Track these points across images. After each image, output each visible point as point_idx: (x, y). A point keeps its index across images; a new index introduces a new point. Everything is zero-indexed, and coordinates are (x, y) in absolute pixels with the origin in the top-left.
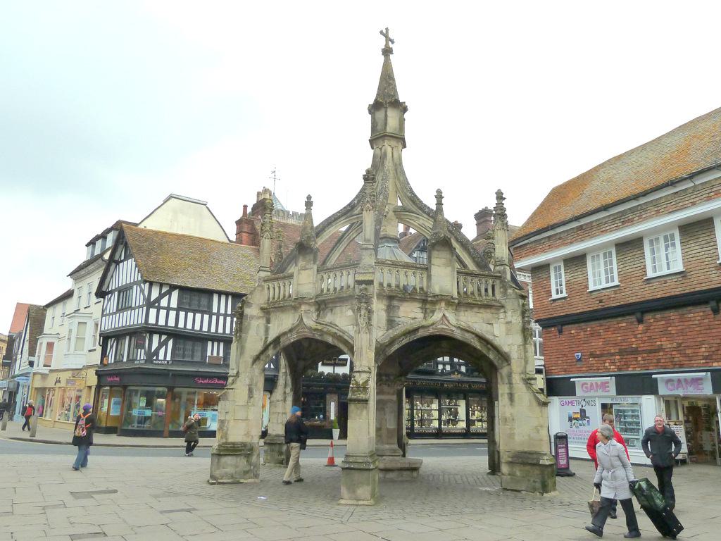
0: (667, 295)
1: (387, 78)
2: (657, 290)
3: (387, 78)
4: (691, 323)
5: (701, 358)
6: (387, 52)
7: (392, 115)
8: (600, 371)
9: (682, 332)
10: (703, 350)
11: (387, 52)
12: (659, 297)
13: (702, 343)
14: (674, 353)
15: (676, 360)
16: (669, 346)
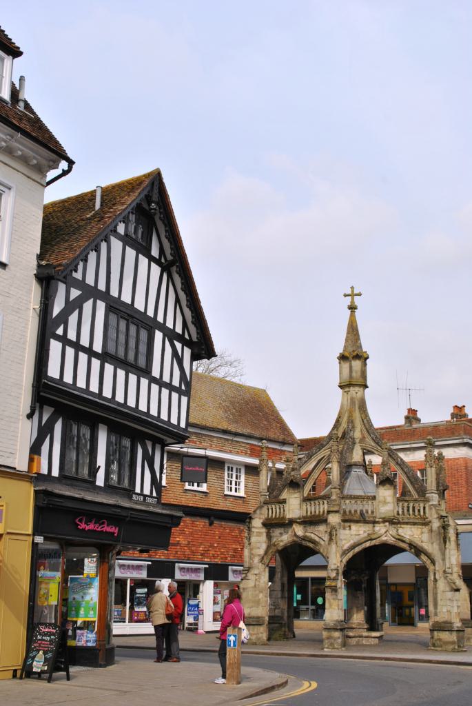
0: (196, 506)
1: (353, 330)
2: (189, 500)
3: (353, 330)
4: (197, 528)
5: (199, 554)
6: (352, 308)
7: (357, 364)
8: (135, 555)
9: (191, 534)
10: (201, 549)
11: (352, 308)
12: (190, 505)
13: (201, 544)
14: (186, 548)
15: (186, 553)
16: (184, 542)
